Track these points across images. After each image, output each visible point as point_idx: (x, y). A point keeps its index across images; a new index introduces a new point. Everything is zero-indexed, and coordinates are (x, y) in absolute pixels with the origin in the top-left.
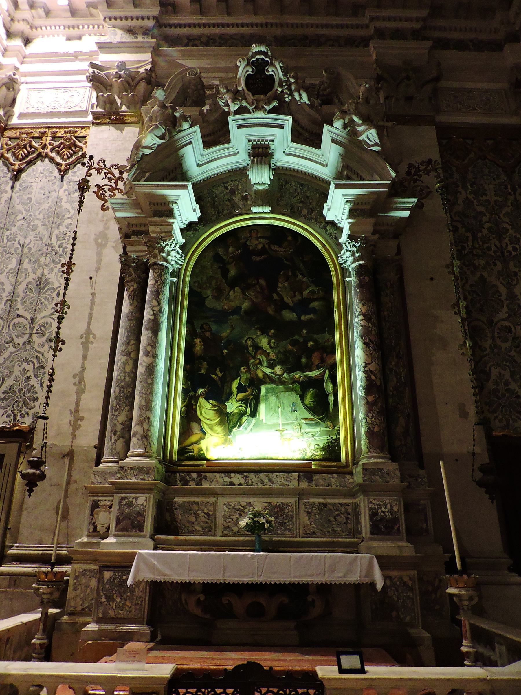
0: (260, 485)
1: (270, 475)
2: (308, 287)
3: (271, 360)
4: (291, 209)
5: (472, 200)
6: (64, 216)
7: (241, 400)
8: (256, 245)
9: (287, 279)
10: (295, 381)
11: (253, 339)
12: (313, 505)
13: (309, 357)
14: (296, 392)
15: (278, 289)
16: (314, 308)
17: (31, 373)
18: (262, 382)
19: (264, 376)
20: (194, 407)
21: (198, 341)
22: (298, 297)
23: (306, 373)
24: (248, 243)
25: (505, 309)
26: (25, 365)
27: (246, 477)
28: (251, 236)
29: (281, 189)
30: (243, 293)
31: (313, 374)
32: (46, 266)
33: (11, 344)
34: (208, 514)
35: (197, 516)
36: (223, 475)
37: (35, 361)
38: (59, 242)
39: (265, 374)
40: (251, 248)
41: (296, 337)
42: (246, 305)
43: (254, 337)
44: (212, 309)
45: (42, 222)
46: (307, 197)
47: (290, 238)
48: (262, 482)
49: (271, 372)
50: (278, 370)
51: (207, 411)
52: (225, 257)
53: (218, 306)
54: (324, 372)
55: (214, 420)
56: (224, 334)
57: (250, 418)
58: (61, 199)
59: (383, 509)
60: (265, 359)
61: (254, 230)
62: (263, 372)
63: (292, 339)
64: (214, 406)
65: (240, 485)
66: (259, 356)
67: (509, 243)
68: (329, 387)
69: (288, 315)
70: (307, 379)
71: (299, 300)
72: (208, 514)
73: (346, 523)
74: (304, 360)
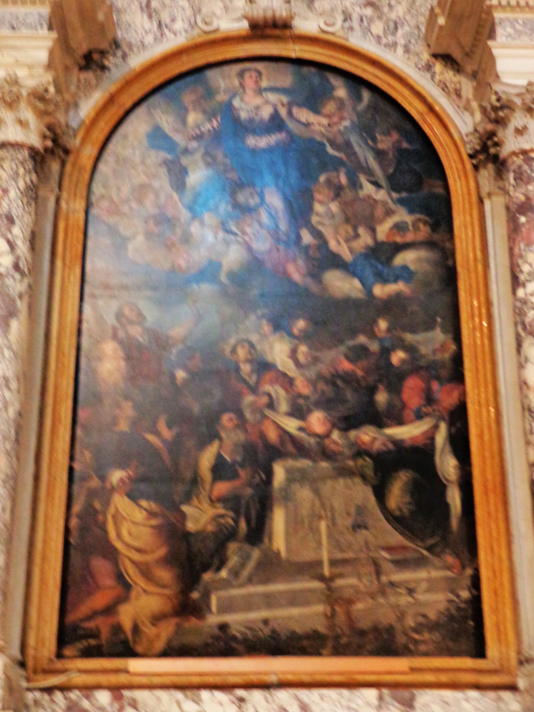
1: (304, 694)
2: (389, 213)
3: (300, 396)
4: (345, 20)
7: (223, 500)
8: (257, 108)
11: (252, 346)
14: (364, 477)
15: (314, 219)
16: (405, 268)
19: (280, 437)
20: (100, 517)
24: (236, 103)
28: (242, 86)
39: (283, 432)
41: (362, 339)
43: (254, 338)
49: (301, 429)
51: (134, 529)
54: (436, 427)
55: (153, 552)
57: (247, 547)
60: (282, 392)
61: (249, 70)
62: (279, 427)
63: (351, 343)
64: (151, 514)
66: (268, 388)
70: (391, 446)
71: (368, 248)
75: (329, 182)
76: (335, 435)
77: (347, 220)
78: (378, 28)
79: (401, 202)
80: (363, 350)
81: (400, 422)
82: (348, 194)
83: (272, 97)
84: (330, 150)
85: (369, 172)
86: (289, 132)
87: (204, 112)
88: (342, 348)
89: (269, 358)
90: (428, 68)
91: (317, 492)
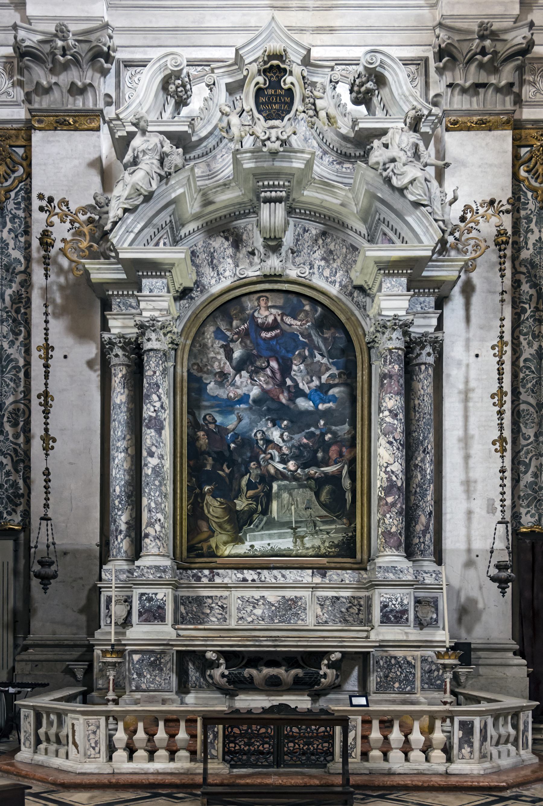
0: (274, 581)
2: (328, 369)
3: (284, 454)
4: (310, 269)
6: (14, 268)
7: (251, 497)
8: (266, 317)
9: (304, 359)
10: (309, 478)
11: (263, 433)
12: (327, 598)
13: (326, 451)
14: (311, 489)
15: (293, 373)
16: (334, 396)
18: (273, 478)
19: (276, 472)
20: (201, 505)
21: (201, 434)
22: (316, 382)
23: (322, 469)
24: (256, 314)
27: (259, 573)
28: (259, 305)
29: (298, 240)
30: (251, 378)
31: (331, 469)
32: (5, 337)
34: (222, 607)
35: (211, 609)
36: (236, 572)
38: (15, 306)
39: (277, 470)
40: (260, 321)
41: (312, 429)
42: (255, 392)
43: (264, 429)
44: (216, 398)
46: (331, 252)
47: (307, 308)
48: (276, 578)
49: (284, 468)
50: (291, 465)
51: (214, 509)
52: (228, 333)
53: (222, 393)
54: (343, 467)
55: (223, 518)
56: (231, 427)
57: (261, 516)
58: (7, 244)
59: (394, 602)
60: (277, 453)
61: (263, 296)
62: (275, 468)
63: (307, 431)
64: (222, 504)
65: (253, 580)
68: (346, 483)
69: (303, 404)
70: (323, 475)
71: (316, 386)
72: (222, 607)
73: (358, 614)
74: (320, 455)
75: (299, 354)
76: (299, 471)
77: (308, 373)
78: (327, 273)
79: (333, 364)
80: (313, 433)
81: (327, 465)
82: (309, 360)
83: (273, 311)
84: (301, 338)
85: (319, 349)
86: (282, 330)
87: (241, 320)
88: (303, 433)
89: (271, 438)
90: (351, 294)
91: (291, 494)
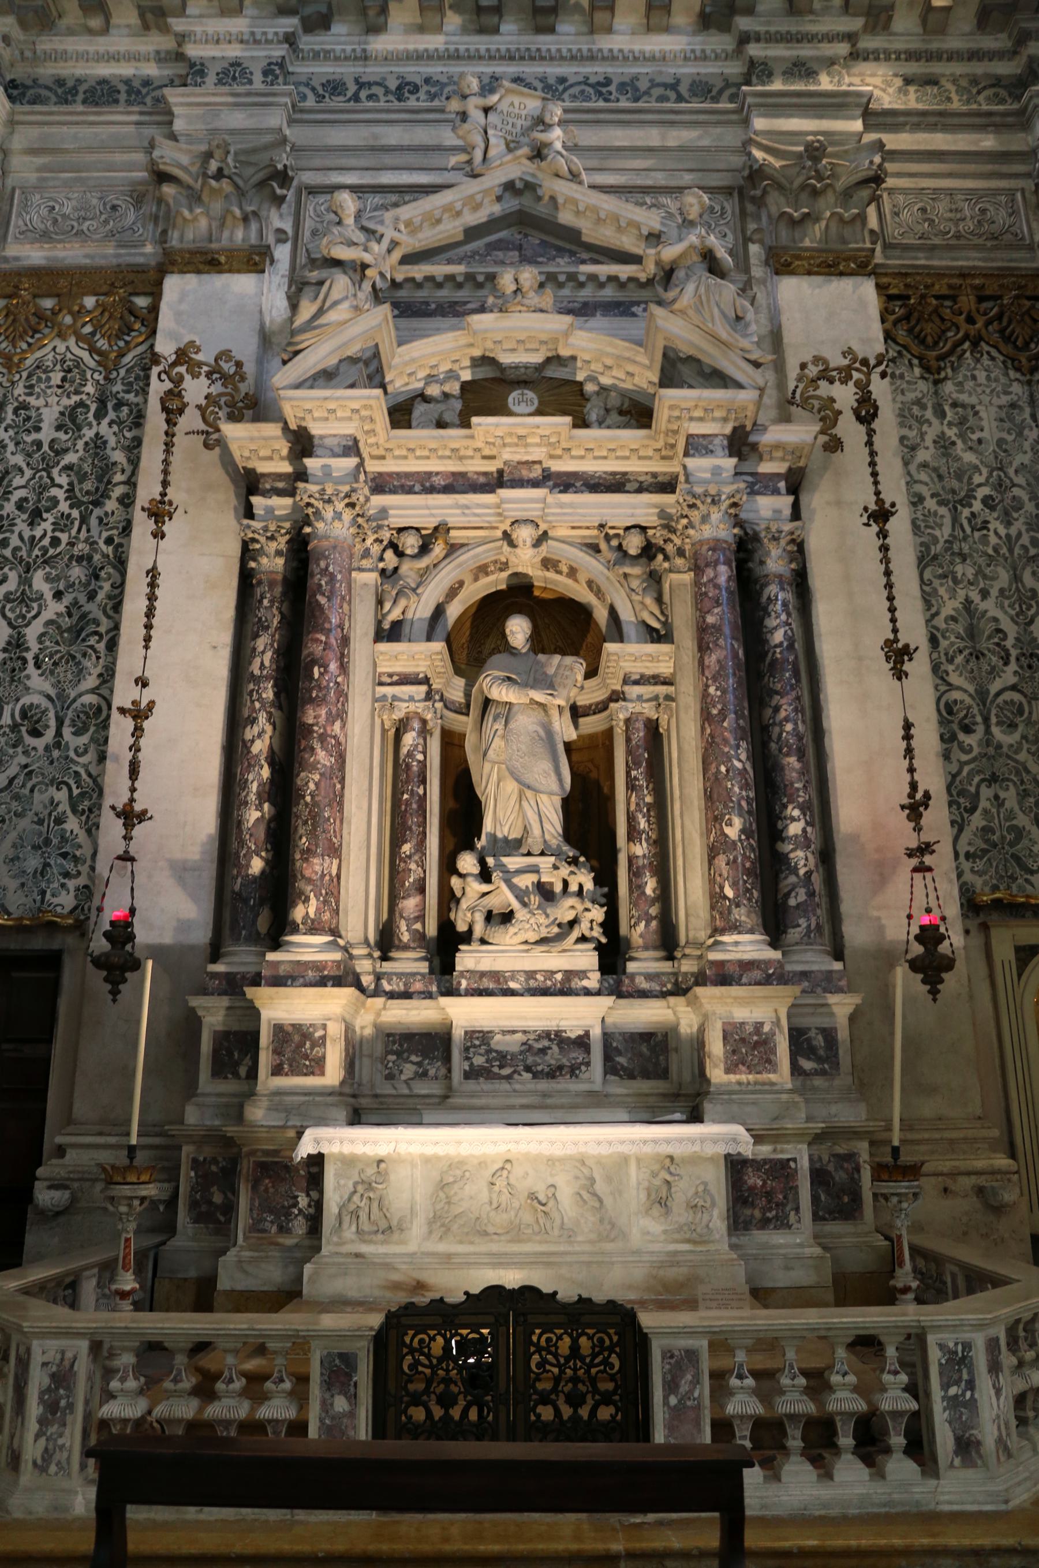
5: (954, 438)
17: (65, 807)
25: (1013, 666)
26: (52, 790)
33: (20, 749)
37: (71, 782)
38: (105, 535)
45: (67, 491)
58: (105, 442)
67: (1023, 529)
